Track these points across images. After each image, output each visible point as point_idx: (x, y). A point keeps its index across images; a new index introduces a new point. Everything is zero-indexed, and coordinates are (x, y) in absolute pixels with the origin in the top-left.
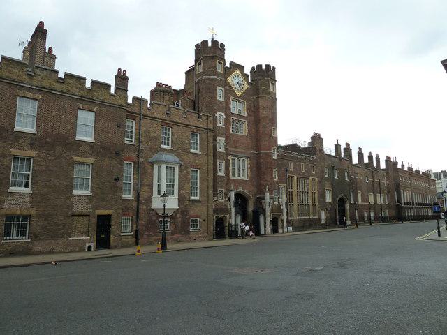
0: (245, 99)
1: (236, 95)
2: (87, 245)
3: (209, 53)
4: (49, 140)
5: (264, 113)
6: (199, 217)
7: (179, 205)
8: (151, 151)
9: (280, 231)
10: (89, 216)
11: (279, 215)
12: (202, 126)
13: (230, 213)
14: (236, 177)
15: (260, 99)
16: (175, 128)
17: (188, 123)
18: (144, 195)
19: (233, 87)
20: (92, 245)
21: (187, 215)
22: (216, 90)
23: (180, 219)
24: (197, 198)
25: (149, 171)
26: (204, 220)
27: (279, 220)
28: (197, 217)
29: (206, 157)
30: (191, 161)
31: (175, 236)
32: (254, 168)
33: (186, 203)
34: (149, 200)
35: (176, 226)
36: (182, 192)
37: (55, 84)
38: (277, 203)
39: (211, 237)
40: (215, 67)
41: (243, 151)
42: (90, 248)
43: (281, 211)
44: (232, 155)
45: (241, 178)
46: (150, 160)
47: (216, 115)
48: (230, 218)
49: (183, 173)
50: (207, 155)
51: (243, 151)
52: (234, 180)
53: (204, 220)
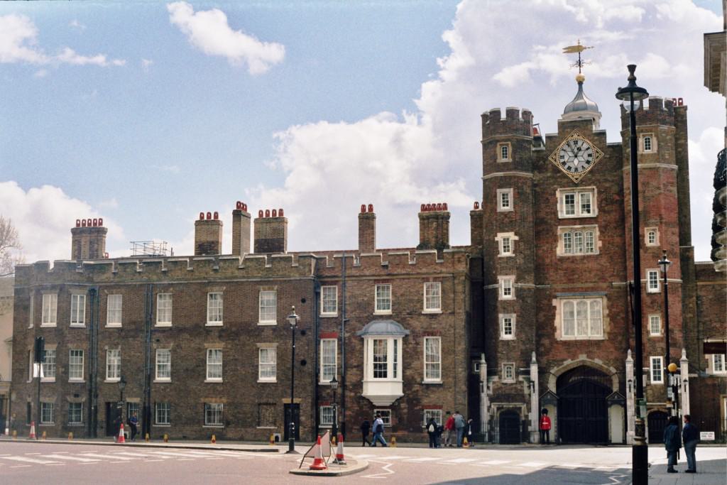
0: (593, 183)
2: (275, 435)
4: (234, 329)
6: (440, 407)
7: (404, 392)
8: (360, 321)
10: (275, 404)
13: (529, 403)
16: (397, 282)
17: (419, 271)
18: (351, 378)
20: (279, 435)
21: (417, 405)
22: (496, 196)
23: (405, 411)
24: (438, 380)
25: (358, 348)
28: (436, 407)
29: (451, 318)
30: (425, 326)
31: (400, 433)
32: (622, 315)
33: (416, 387)
34: (359, 385)
35: (401, 420)
36: (408, 372)
37: (236, 271)
38: (662, 382)
40: (495, 157)
42: (277, 438)
46: (359, 333)
47: (496, 239)
48: (529, 410)
49: (411, 346)
50: (453, 313)
52: (567, 344)
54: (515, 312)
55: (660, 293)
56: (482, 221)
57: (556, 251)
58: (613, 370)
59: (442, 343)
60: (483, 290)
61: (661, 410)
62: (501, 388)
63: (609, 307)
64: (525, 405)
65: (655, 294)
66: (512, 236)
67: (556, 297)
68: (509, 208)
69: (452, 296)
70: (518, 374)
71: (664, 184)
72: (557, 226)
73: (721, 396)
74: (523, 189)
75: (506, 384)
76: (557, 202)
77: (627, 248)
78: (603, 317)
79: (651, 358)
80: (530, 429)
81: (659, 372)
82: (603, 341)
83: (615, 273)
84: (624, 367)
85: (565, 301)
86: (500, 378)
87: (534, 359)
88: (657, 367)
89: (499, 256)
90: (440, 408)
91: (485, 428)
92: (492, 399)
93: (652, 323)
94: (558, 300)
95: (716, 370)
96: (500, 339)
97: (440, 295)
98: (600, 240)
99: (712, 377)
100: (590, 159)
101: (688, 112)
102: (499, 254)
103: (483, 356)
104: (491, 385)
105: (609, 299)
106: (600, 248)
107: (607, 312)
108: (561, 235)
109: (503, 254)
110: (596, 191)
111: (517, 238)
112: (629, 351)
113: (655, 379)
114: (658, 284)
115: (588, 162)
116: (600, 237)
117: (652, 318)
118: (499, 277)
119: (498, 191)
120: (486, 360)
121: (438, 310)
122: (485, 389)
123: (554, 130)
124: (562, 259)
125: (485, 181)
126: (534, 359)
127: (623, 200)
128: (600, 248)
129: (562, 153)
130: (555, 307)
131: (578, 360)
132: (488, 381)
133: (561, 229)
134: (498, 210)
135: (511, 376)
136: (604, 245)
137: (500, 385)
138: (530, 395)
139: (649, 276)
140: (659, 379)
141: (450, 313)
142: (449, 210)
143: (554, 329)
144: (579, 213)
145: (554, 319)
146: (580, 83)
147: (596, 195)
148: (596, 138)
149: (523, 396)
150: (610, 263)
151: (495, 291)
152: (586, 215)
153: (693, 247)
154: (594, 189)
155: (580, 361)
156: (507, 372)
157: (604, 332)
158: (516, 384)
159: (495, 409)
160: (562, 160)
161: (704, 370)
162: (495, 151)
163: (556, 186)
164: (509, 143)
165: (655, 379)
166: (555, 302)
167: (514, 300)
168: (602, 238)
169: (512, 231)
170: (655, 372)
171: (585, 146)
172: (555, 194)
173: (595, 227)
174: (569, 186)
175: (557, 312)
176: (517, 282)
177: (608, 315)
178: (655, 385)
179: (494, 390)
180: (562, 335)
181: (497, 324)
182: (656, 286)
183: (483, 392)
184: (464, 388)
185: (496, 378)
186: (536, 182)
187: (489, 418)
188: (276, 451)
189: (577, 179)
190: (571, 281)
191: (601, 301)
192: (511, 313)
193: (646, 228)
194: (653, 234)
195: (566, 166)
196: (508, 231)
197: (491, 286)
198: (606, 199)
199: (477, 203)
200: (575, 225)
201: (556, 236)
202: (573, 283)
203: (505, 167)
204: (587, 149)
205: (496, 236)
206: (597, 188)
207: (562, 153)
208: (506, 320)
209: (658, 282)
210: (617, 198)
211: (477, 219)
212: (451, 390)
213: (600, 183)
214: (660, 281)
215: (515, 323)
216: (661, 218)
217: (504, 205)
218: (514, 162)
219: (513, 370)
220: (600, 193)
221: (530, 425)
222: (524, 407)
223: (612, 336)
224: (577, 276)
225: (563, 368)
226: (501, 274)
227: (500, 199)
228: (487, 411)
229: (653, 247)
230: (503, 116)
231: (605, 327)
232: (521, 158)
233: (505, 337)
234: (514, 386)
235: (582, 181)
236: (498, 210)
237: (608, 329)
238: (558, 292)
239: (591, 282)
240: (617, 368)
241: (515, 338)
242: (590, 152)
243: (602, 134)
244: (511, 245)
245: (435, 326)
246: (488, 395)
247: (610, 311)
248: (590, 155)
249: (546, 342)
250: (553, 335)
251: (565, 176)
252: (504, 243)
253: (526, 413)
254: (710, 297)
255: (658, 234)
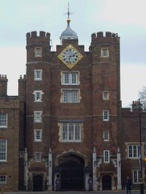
1: (68, 69)
3: (37, 42)
5: (96, 79)
6: (6, 174)
9: (113, 188)
11: (112, 174)
12: (9, 107)
13: (47, 172)
14: (67, 140)
15: (93, 67)
19: (64, 62)
22: (34, 73)
24: (5, 161)
26: (10, 177)
27: (113, 178)
38: (109, 162)
39: (17, 189)
40: (34, 54)
41: (76, 117)
43: (115, 169)
44: (62, 122)
45: (74, 140)
47: (33, 93)
48: (48, 175)
50: (13, 128)
51: (76, 117)
53: (10, 177)
54: (42, 129)
55: (109, 122)
56: (24, 84)
57: (60, 100)
58: (85, 156)
59: (7, 143)
60: (25, 118)
61: (108, 175)
62: (35, 164)
63: (84, 127)
64: (46, 173)
65: (106, 122)
66: (41, 93)
67: (59, 122)
68: (40, 79)
69: (13, 120)
70: (43, 157)
71: (111, 72)
72: (61, 89)
73: (132, 168)
74: (46, 70)
75: (37, 163)
76: (61, 77)
77: (93, 100)
78: (81, 132)
79: (104, 151)
80: (48, 184)
81: (108, 158)
82: (81, 143)
83: (87, 112)
84: (91, 155)
85: (63, 124)
86: (34, 160)
87: (50, 151)
88: (107, 155)
89: (35, 101)
90: (6, 175)
91: (26, 184)
92: (30, 170)
93: (105, 135)
94: (61, 123)
95: (130, 157)
96: (35, 141)
97: (7, 119)
98: (80, 96)
99: (129, 160)
100: (77, 58)
101: (121, 39)
102: (34, 100)
103: (26, 149)
104: (29, 163)
105: (84, 124)
106: (80, 100)
107: (83, 129)
108: (62, 93)
109: (36, 101)
110: (79, 73)
111: (43, 93)
112: (94, 148)
113: (106, 161)
114: (108, 117)
115: (76, 60)
116: (80, 94)
117: (105, 133)
118: (35, 112)
119: (35, 70)
120: (27, 151)
121: (6, 127)
122: (27, 165)
123: (60, 43)
124: (63, 104)
125: (27, 65)
126: (50, 151)
127: (91, 79)
128: (80, 100)
129: (64, 54)
130: (59, 127)
131: (69, 152)
132: (28, 162)
133: (63, 90)
134: (35, 80)
135: (39, 159)
136: (82, 98)
137: (34, 163)
138: (48, 168)
139: (104, 113)
140: (108, 161)
141: (12, 128)
142: (7, 78)
143: (59, 137)
144: (70, 83)
145: (59, 132)
146: (69, 22)
147: (79, 75)
148: (80, 49)
149: (45, 168)
150: (85, 107)
151: (32, 119)
152: (74, 84)
153: (121, 101)
154: (78, 72)
155: (70, 152)
156: (37, 157)
157: (81, 139)
158: (42, 162)
159: (31, 175)
160: (63, 58)
161: (125, 157)
162: (34, 51)
163: (61, 70)
164: (41, 48)
165: (106, 161)
166: (59, 124)
167: (41, 123)
168: (82, 95)
169: (41, 90)
170: (105, 157)
171: (75, 52)
172: (60, 74)
173: (78, 90)
174: (67, 71)
175: (60, 129)
176: (43, 114)
177: (84, 131)
178: (106, 163)
179: (31, 165)
180: (61, 140)
181: (33, 134)
182: (107, 118)
183: (26, 166)
184: (18, 164)
185: (32, 160)
186: (51, 67)
187: (28, 179)
188: (119, 166)
189: (70, 67)
190: (66, 114)
191: (80, 124)
192: (40, 129)
193: (103, 92)
194: (106, 94)
195: (66, 61)
196: (40, 90)
197: (30, 116)
198: (83, 77)
199: (21, 75)
200: (69, 88)
201: (60, 93)
202: (68, 115)
203: (38, 59)
204: (76, 53)
205: (34, 92)
206: (80, 72)
207: (64, 54)
208: (37, 132)
209: (108, 116)
210: (88, 77)
211: (22, 83)
212: (11, 165)
213: (81, 69)
214: (109, 116)
215: (41, 134)
216: (110, 88)
217: (37, 78)
218: (43, 57)
219: (40, 156)
220: (81, 74)
221: (48, 182)
222: (45, 174)
223: (85, 141)
224: (69, 112)
225: (62, 155)
226: (35, 110)
227: (36, 74)
228: (28, 175)
229: (106, 101)
230: (38, 35)
231: (82, 137)
232: (45, 55)
233: (36, 140)
234: (41, 163)
235: (73, 68)
236: (35, 80)
237: (83, 138)
238: (60, 119)
239: (76, 115)
240: (87, 155)
241: (41, 141)
242: (77, 55)
243: (83, 47)
244: (41, 97)
245: (4, 134)
246: (28, 168)
247: (84, 129)
248: (77, 56)
249: (54, 143)
250: (58, 140)
251: (65, 65)
252: (37, 96)
253: (46, 176)
254: (128, 124)
255: (108, 95)
